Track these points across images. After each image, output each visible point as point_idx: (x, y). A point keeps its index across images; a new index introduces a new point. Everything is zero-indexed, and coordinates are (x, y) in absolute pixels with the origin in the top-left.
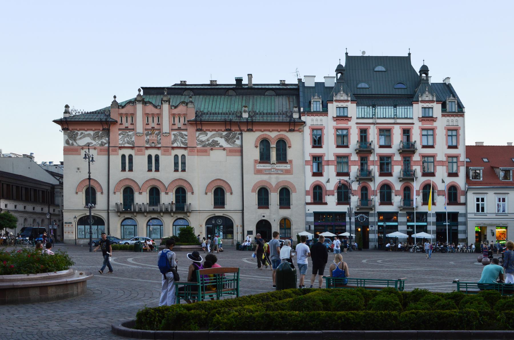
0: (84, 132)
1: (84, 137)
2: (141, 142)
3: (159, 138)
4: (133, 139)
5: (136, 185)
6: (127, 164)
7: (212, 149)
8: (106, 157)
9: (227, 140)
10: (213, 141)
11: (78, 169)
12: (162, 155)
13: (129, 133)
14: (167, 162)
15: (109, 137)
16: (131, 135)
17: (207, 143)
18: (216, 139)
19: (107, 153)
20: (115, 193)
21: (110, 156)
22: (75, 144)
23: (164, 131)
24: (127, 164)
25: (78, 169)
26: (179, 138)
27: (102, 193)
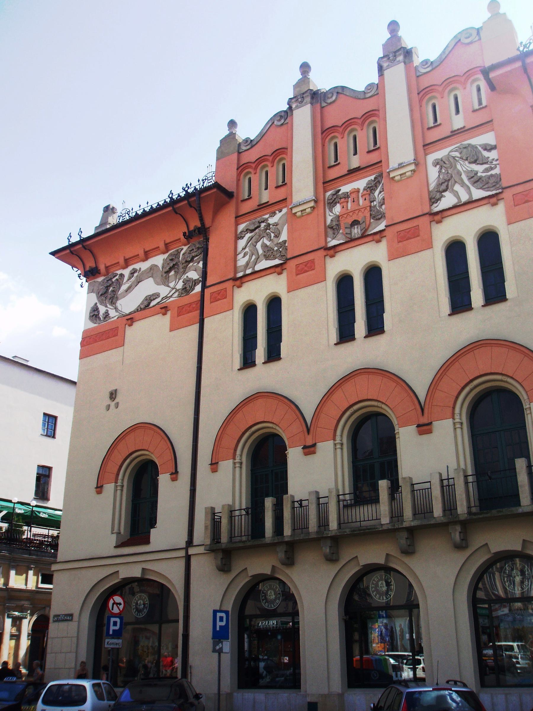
0: (137, 266)
1: (139, 281)
2: (310, 237)
4: (284, 237)
11: (113, 395)
12: (393, 256)
13: (271, 221)
14: (415, 281)
16: (276, 224)
20: (214, 466)
21: (206, 320)
22: (113, 313)
23: (393, 163)
25: (113, 395)
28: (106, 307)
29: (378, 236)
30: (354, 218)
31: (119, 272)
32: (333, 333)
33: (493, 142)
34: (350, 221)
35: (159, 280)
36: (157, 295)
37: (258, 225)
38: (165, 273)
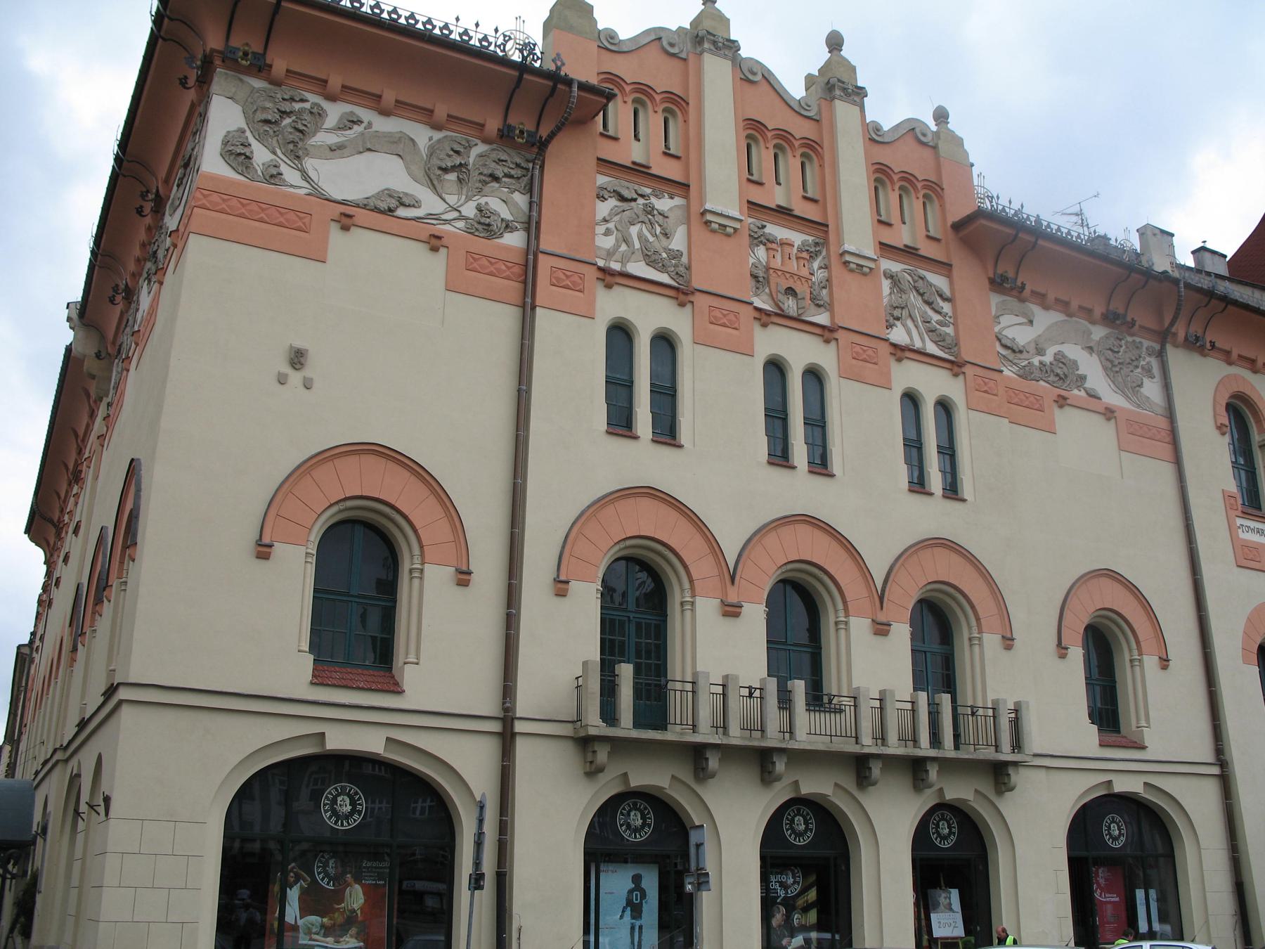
0: (365, 114)
1: (367, 147)
3: (820, 275)
4: (678, 242)
5: (698, 541)
6: (641, 391)
7: (1062, 402)
8: (505, 318)
9: (1112, 369)
10: (1060, 358)
11: (297, 358)
15: (532, 189)
17: (1036, 361)
18: (1073, 352)
19: (514, 287)
20: (561, 587)
22: (290, 175)
24: (641, 391)
25: (297, 358)
26: (914, 299)
27: (463, 577)
28: (274, 153)
29: (827, 333)
30: (790, 284)
31: (313, 98)
32: (760, 445)
33: (947, 293)
34: (785, 284)
35: (420, 174)
36: (416, 204)
37: (635, 196)
38: (440, 168)
